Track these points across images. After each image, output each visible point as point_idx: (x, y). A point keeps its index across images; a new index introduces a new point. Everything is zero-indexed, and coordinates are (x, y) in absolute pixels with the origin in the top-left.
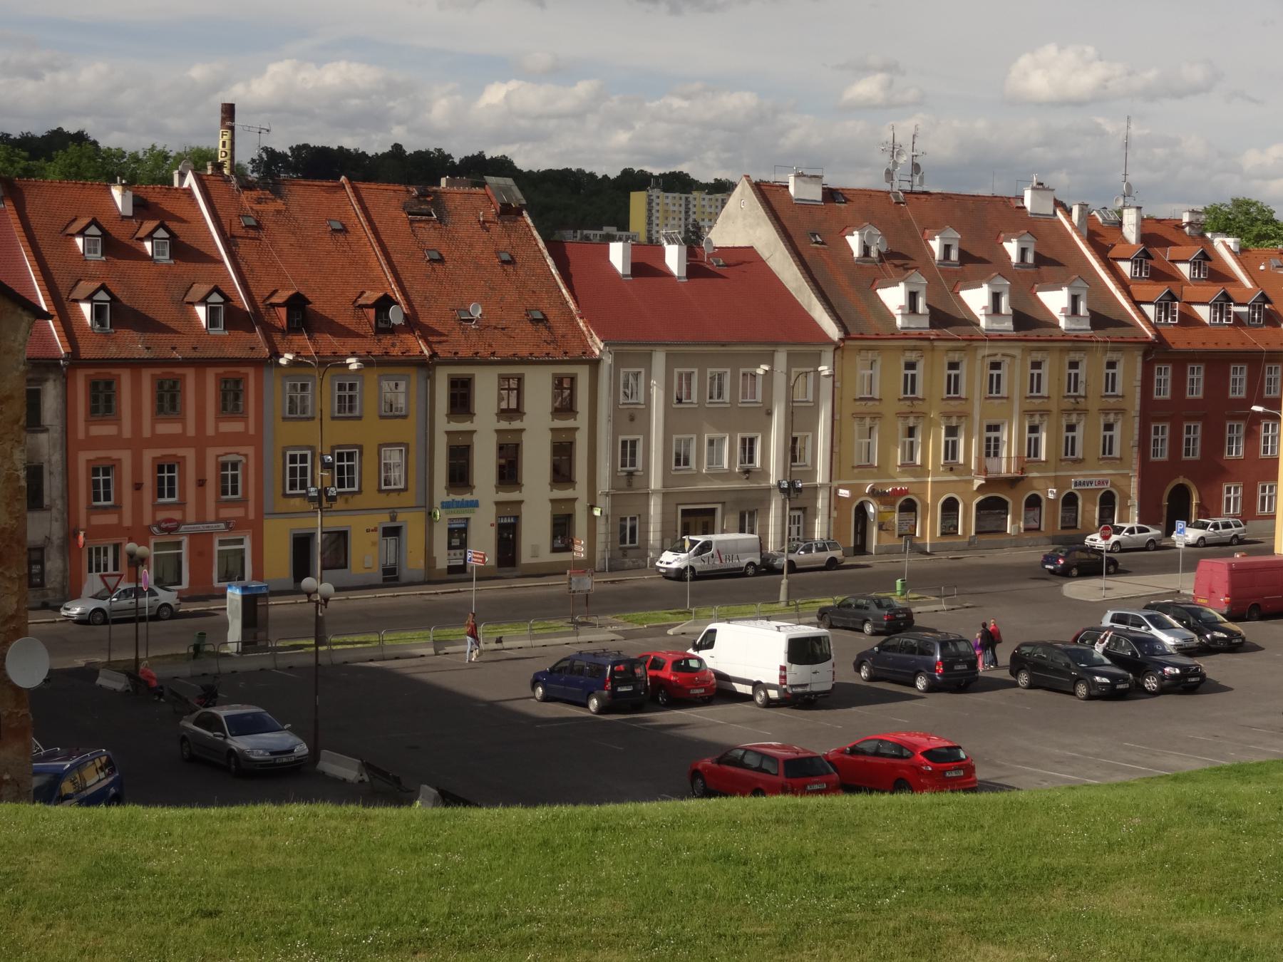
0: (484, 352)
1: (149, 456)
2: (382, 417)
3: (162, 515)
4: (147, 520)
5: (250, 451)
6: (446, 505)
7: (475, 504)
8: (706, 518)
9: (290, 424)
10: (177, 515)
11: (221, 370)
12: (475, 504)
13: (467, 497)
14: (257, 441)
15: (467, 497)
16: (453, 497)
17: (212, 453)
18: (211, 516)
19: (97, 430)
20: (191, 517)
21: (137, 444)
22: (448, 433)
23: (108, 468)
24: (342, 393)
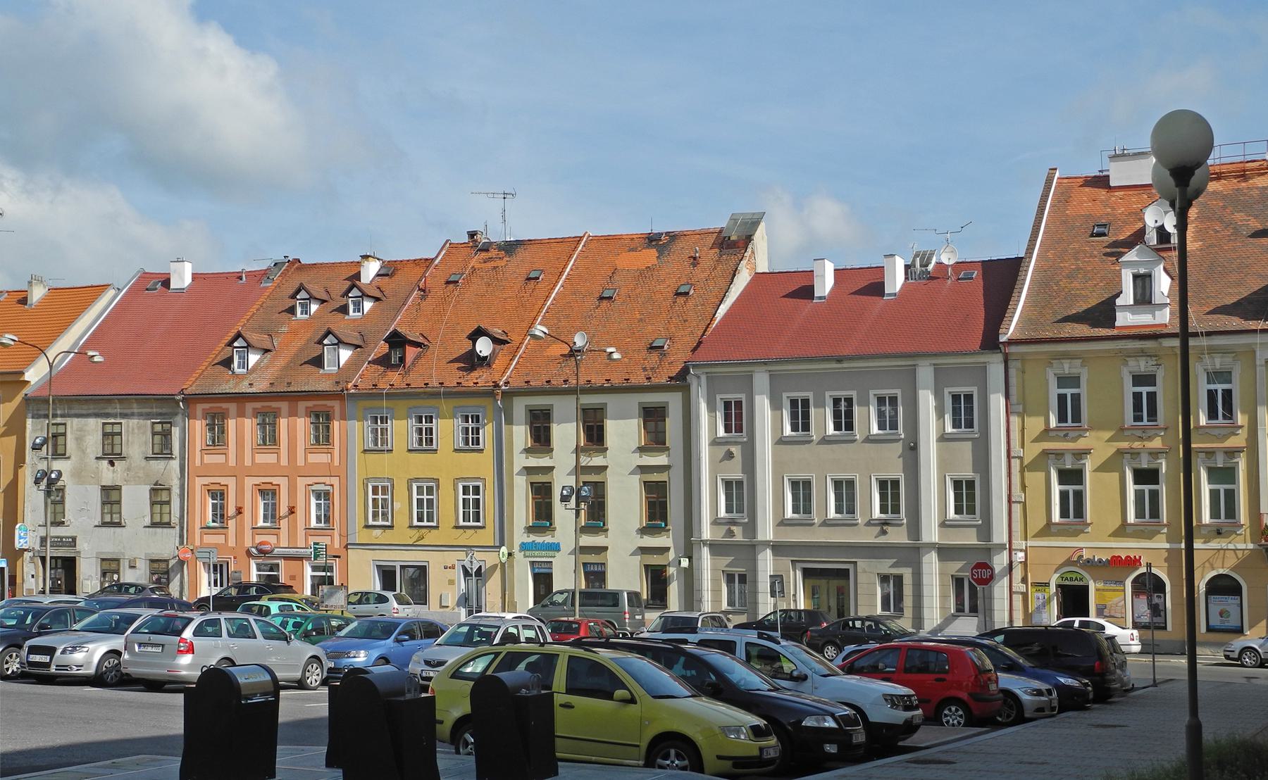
0: (557, 382)
1: (249, 482)
2: (456, 450)
3: (259, 539)
4: (248, 543)
5: (335, 481)
6: (524, 547)
7: (555, 548)
8: (841, 582)
9: (370, 456)
10: (272, 539)
11: (310, 404)
12: (555, 548)
13: (548, 539)
14: (343, 473)
15: (548, 539)
16: (532, 538)
17: (301, 483)
18: (301, 543)
19: (208, 459)
20: (284, 543)
21: (239, 473)
22: (529, 470)
23: (218, 494)
24: (429, 425)
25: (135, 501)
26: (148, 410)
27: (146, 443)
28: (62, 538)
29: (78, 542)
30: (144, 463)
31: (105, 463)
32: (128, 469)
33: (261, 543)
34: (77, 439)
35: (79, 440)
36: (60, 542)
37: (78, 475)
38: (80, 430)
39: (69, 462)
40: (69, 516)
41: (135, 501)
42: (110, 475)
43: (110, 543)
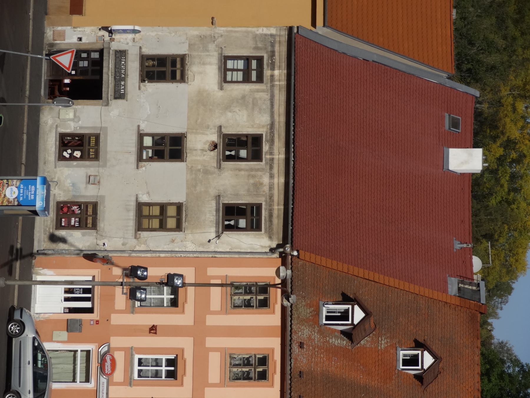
3: (120, 357)
10: (119, 375)
25: (166, 182)
26: (276, 198)
27: (237, 195)
28: (124, 79)
29: (120, 102)
30: (213, 192)
31: (214, 138)
32: (206, 172)
33: (113, 361)
34: (243, 97)
35: (243, 100)
36: (120, 77)
37: (201, 100)
38: (255, 103)
39: (216, 87)
40: (152, 87)
41: (166, 182)
42: (199, 146)
43: (119, 146)
